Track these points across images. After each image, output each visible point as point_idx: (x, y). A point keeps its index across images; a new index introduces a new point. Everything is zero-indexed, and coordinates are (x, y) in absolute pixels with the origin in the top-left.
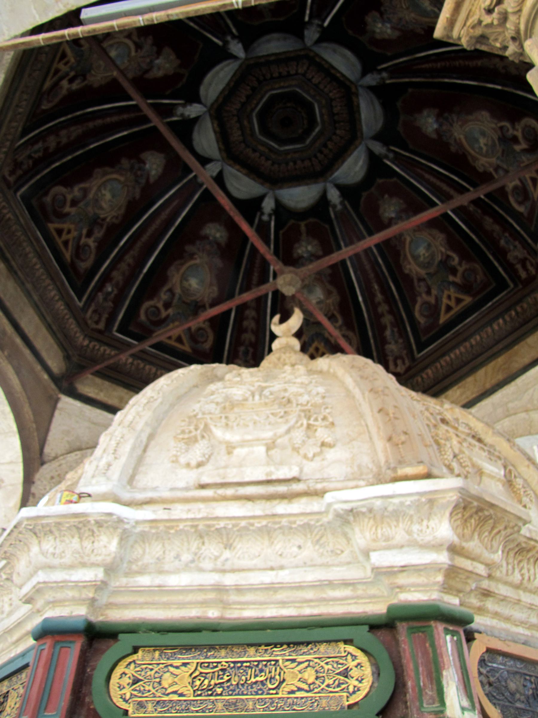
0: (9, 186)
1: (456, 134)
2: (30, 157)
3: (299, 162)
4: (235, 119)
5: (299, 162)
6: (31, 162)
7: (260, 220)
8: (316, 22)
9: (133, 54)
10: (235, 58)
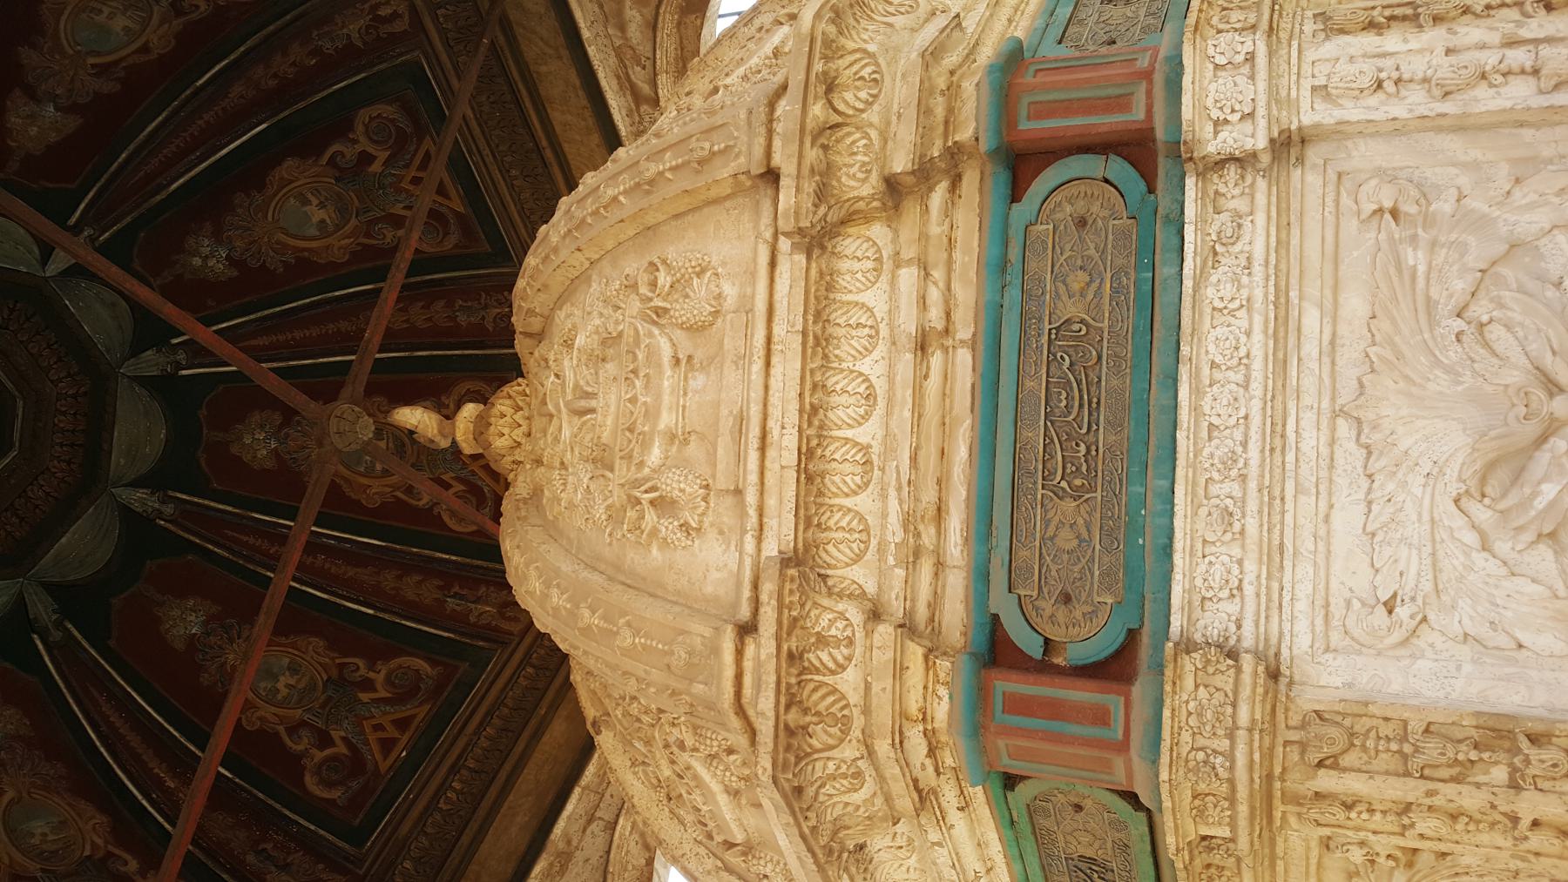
1: (231, 657)
8: (181, 357)
9: (91, 60)
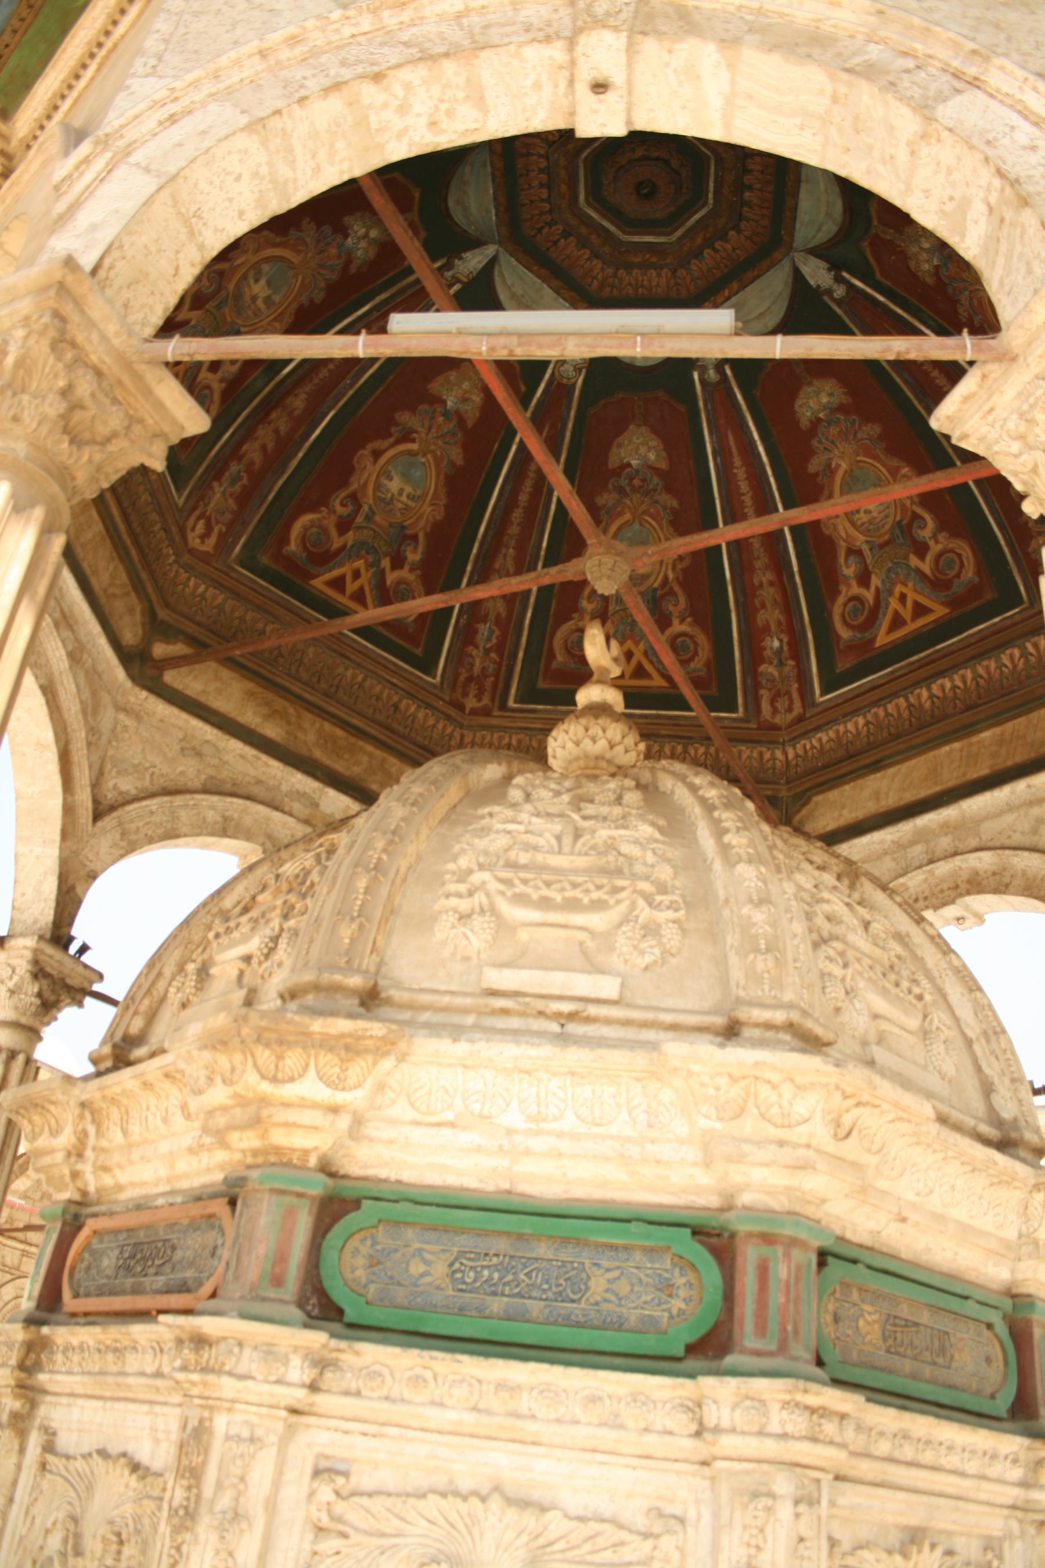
0: (486, 712)
2: (487, 651)
3: (747, 179)
4: (622, 272)
5: (747, 179)
6: (493, 655)
7: (839, 302)
9: (415, 446)
10: (493, 261)
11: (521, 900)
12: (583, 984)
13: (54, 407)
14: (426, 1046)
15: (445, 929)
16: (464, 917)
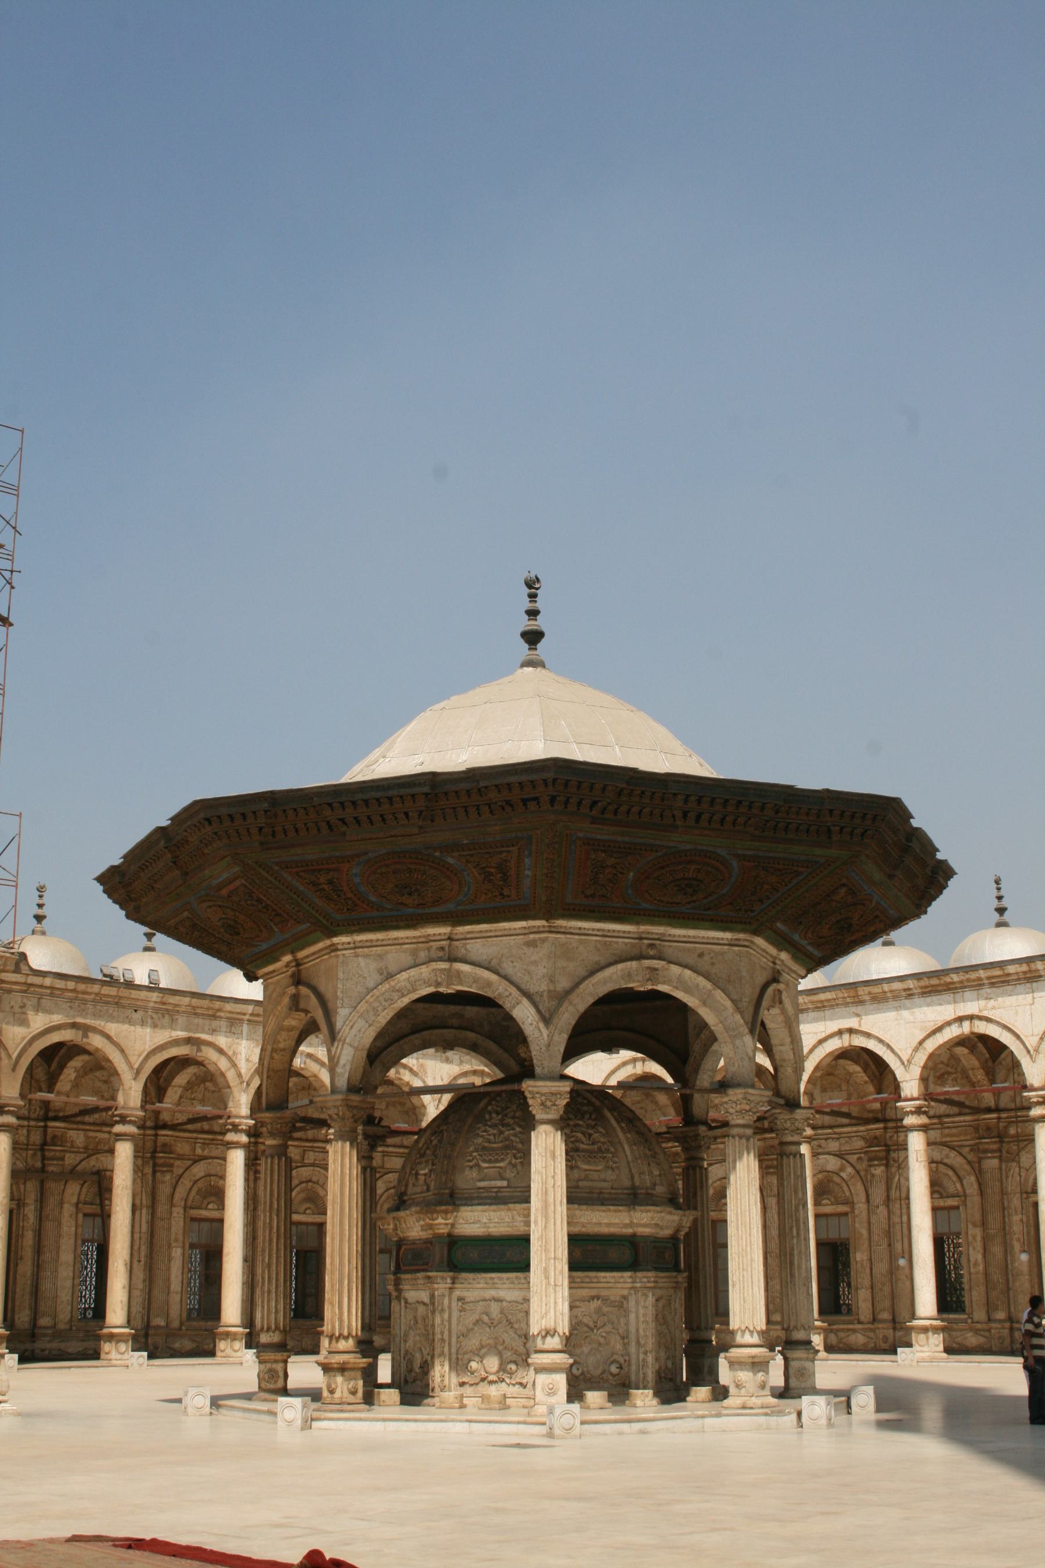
11: (484, 1161)
12: (499, 1183)
13: (351, 1120)
14: (463, 1208)
15: (467, 1172)
16: (471, 1167)
